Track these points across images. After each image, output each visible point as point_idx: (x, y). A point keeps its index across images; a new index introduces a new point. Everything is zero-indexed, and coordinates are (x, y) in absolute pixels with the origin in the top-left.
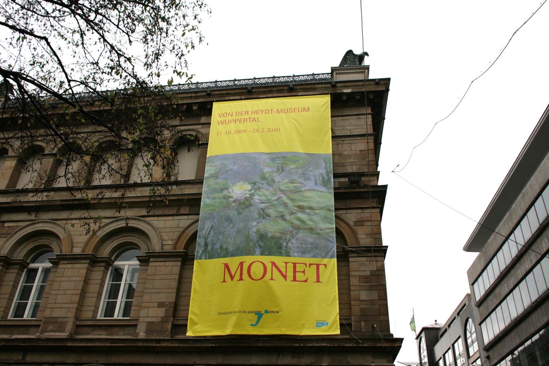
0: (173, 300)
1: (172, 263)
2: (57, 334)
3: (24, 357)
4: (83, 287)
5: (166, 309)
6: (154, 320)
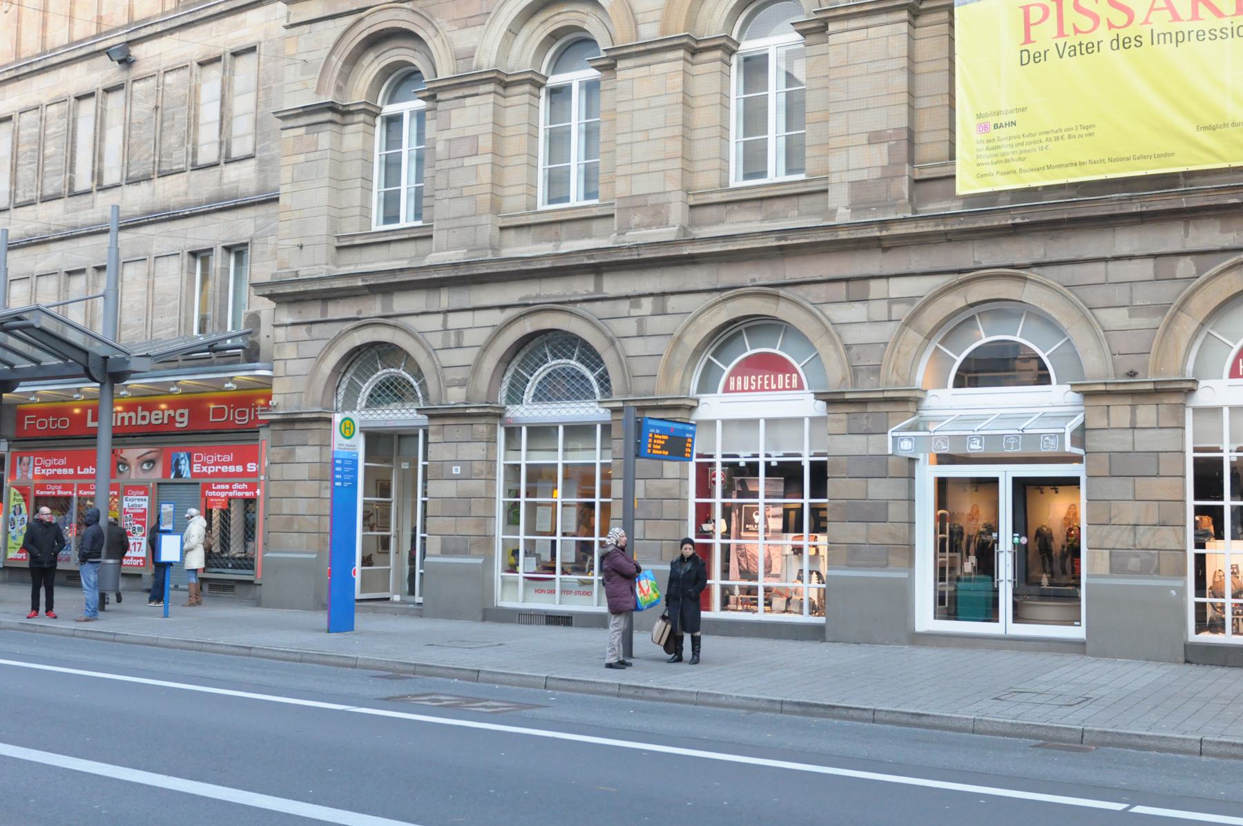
0: (905, 124)
1: (886, 30)
2: (654, 231)
3: (598, 287)
4: (684, 118)
5: (890, 148)
6: (864, 175)
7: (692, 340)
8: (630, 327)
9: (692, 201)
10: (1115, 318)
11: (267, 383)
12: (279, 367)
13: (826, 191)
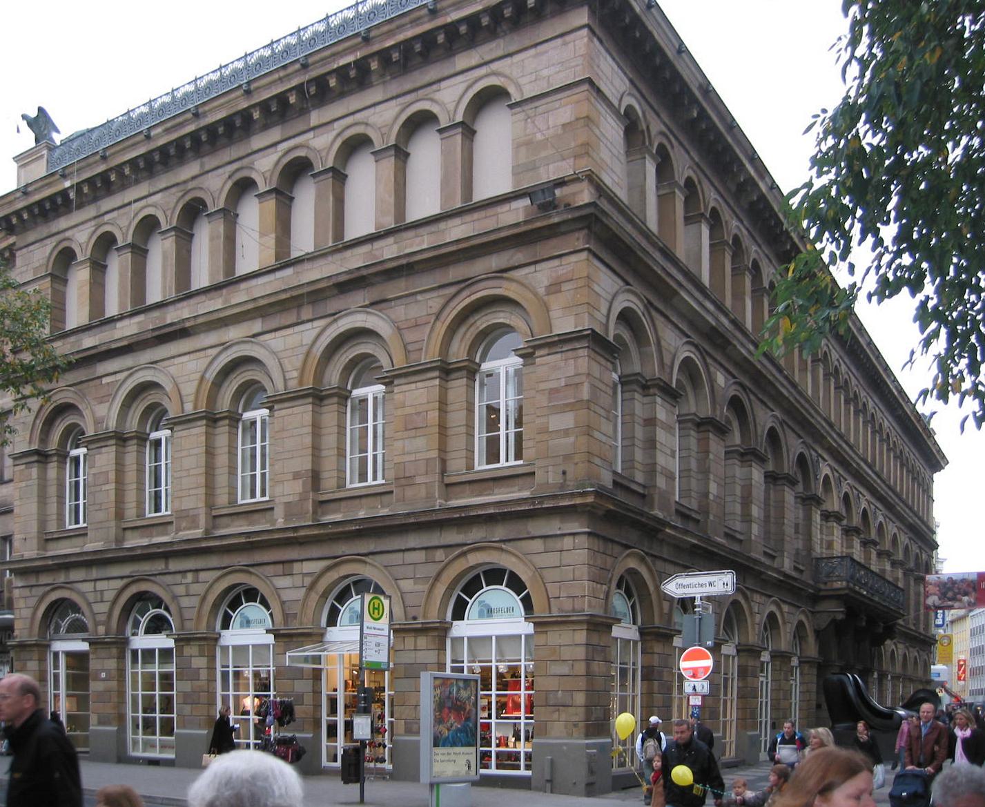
0: (309, 466)
4: (206, 462)
6: (290, 499)
7: (211, 599)
8: (180, 590)
9: (215, 513)
10: (407, 585)
11: (12, 621)
12: (17, 612)
13: (272, 509)
